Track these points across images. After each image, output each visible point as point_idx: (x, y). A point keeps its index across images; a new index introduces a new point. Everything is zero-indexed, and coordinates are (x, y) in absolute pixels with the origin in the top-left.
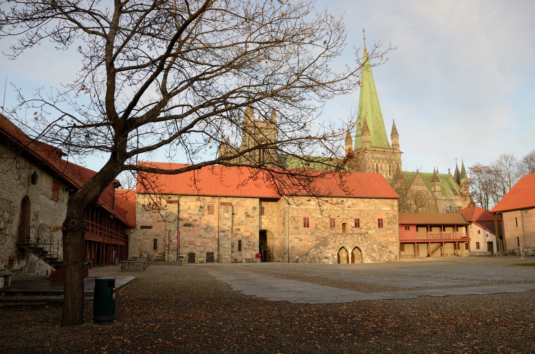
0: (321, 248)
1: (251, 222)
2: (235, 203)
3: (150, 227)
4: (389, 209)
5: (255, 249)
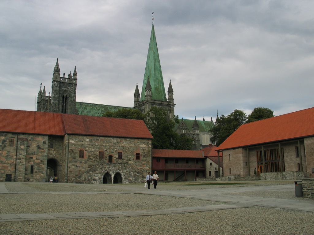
2: (30, 139)
4: (145, 146)
5: (44, 172)
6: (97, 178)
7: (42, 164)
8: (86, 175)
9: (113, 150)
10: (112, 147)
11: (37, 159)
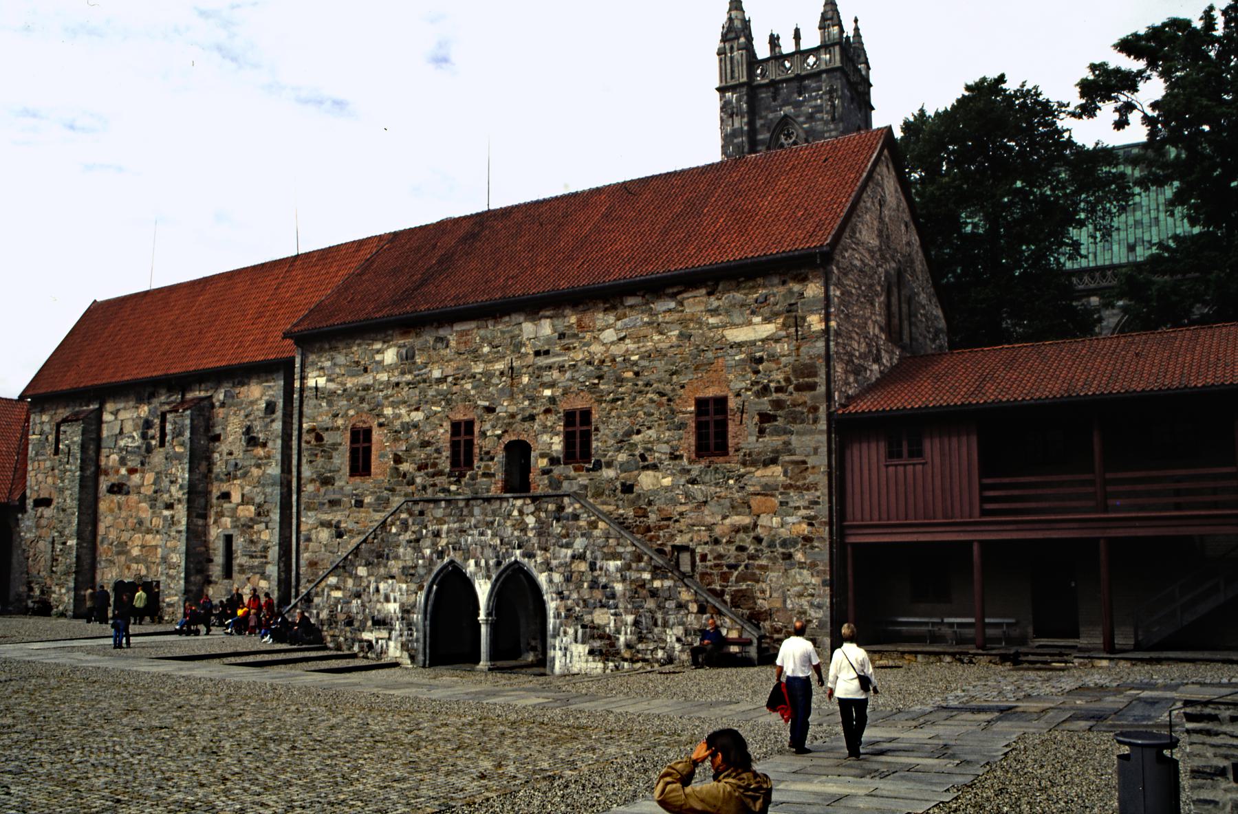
0: (362, 571)
1: (258, 466)
2: (221, 397)
3: (46, 502)
4: (769, 329)
6: (393, 607)
7: (262, 526)
8: (337, 588)
9: (532, 399)
10: (525, 379)
11: (245, 500)
